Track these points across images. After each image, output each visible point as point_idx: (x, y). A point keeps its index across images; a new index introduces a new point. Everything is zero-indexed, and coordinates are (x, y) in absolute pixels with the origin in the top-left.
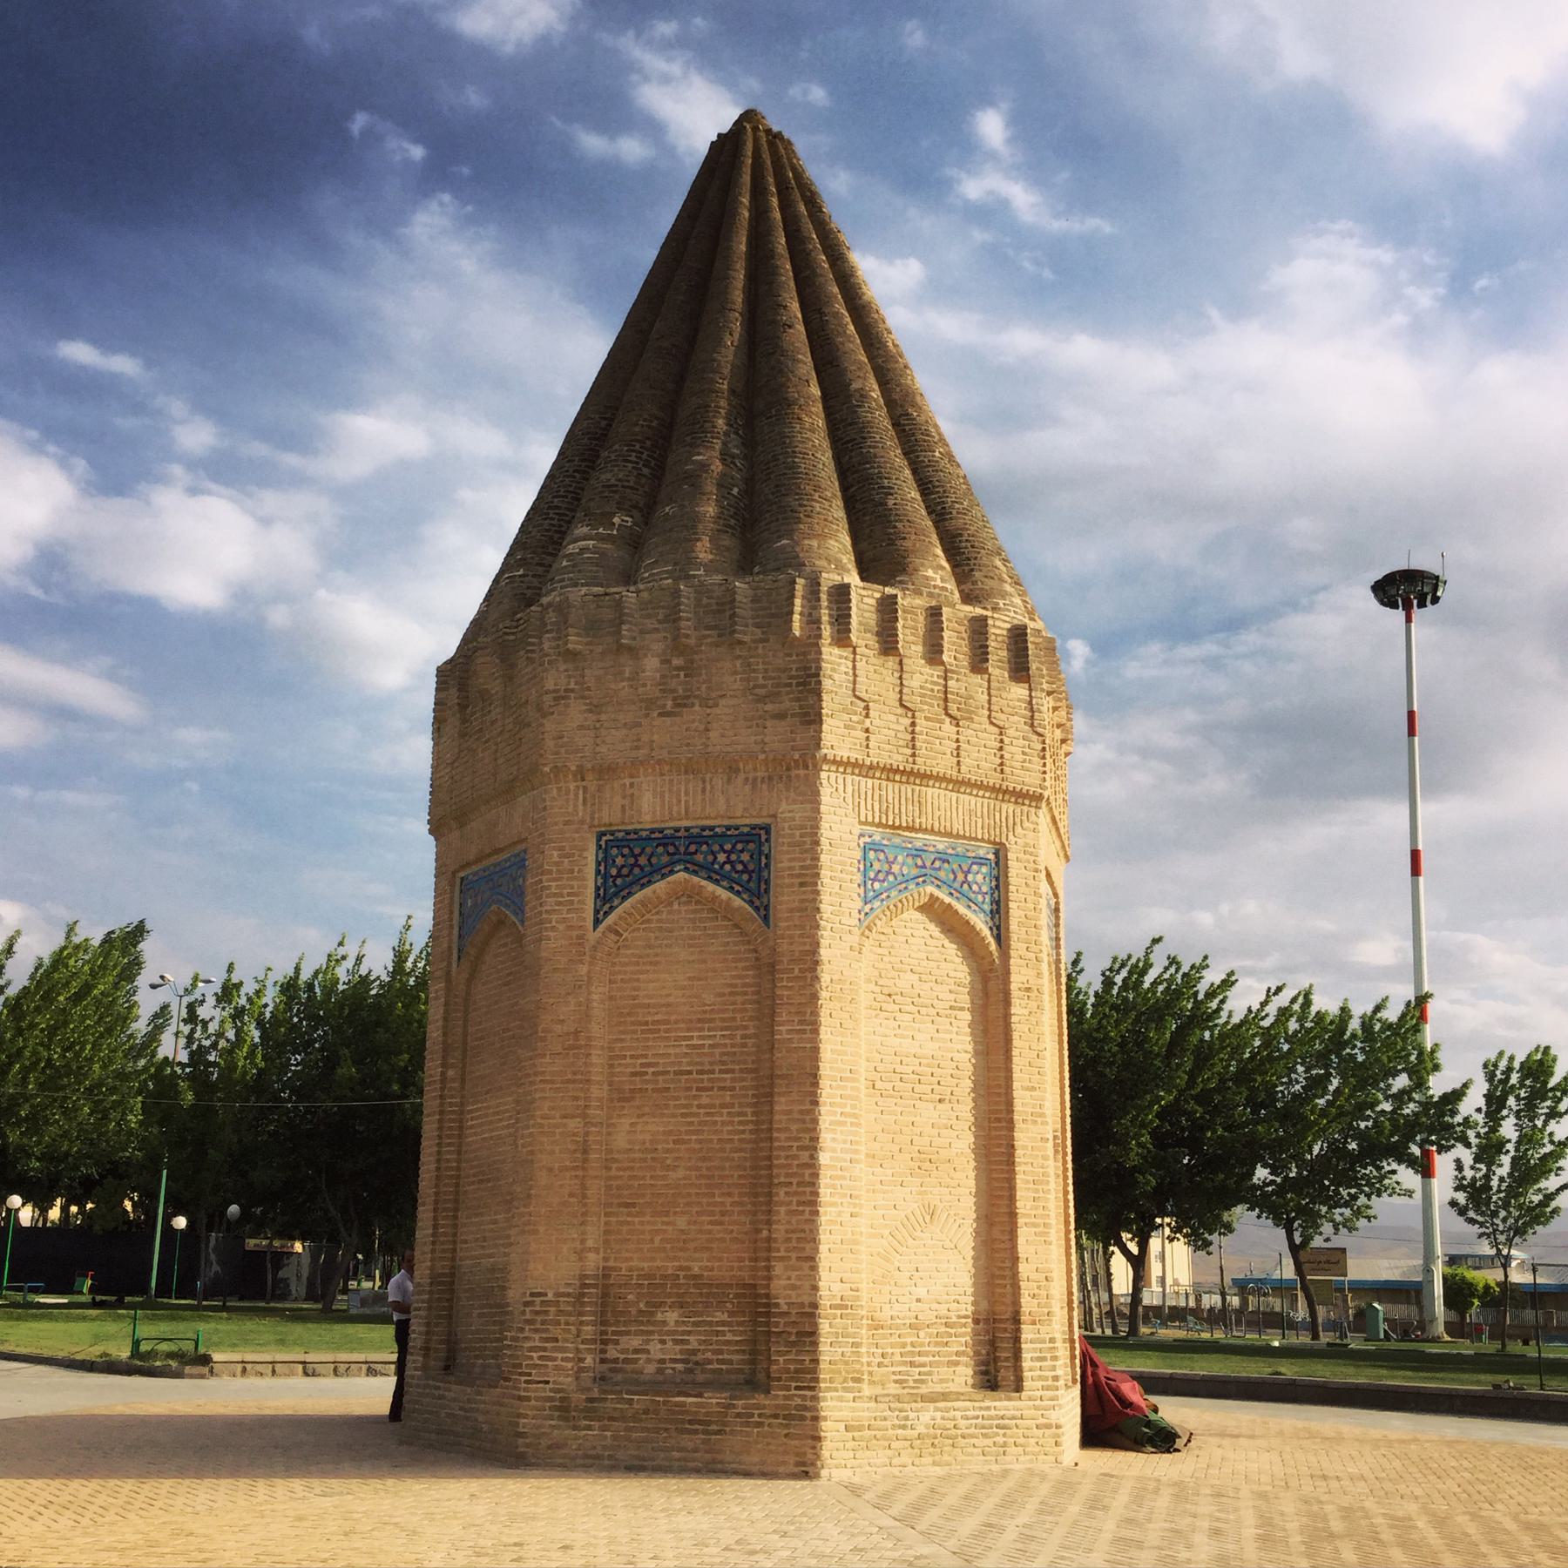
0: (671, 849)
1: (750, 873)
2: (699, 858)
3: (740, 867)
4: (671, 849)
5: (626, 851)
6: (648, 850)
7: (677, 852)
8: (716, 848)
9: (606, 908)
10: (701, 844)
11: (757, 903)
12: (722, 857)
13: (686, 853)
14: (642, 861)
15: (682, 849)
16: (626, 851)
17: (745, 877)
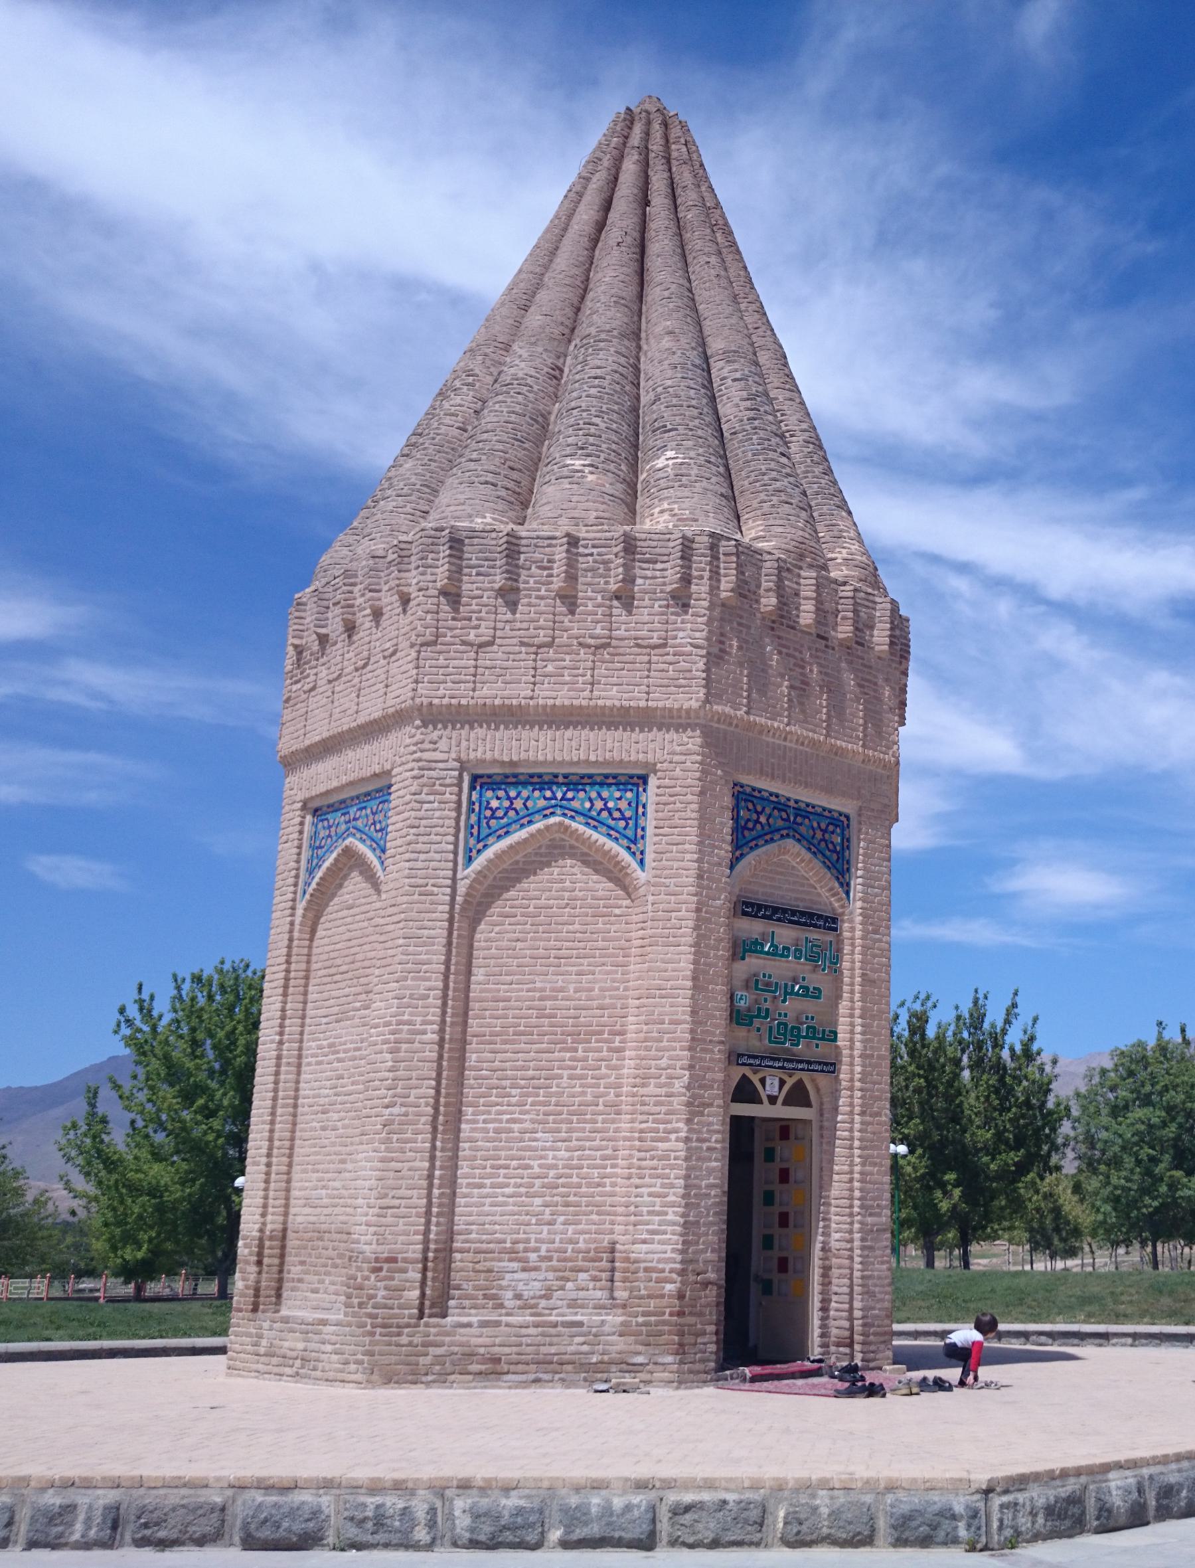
0: (784, 815)
1: (838, 853)
2: (802, 829)
3: (830, 846)
4: (784, 815)
5: (750, 806)
6: (768, 811)
7: (788, 820)
8: (815, 825)
9: (738, 853)
10: (804, 817)
11: (841, 880)
12: (819, 835)
13: (795, 822)
14: (763, 819)
15: (792, 819)
16: (750, 806)
17: (835, 857)
